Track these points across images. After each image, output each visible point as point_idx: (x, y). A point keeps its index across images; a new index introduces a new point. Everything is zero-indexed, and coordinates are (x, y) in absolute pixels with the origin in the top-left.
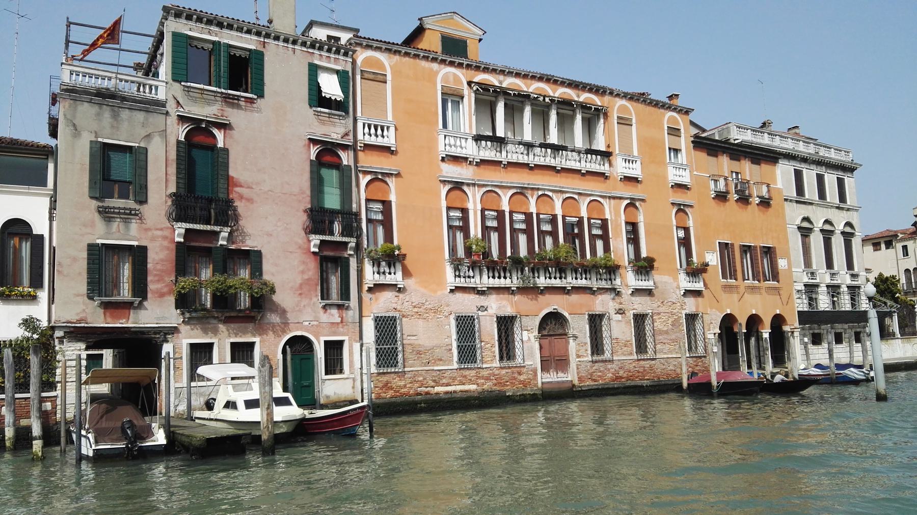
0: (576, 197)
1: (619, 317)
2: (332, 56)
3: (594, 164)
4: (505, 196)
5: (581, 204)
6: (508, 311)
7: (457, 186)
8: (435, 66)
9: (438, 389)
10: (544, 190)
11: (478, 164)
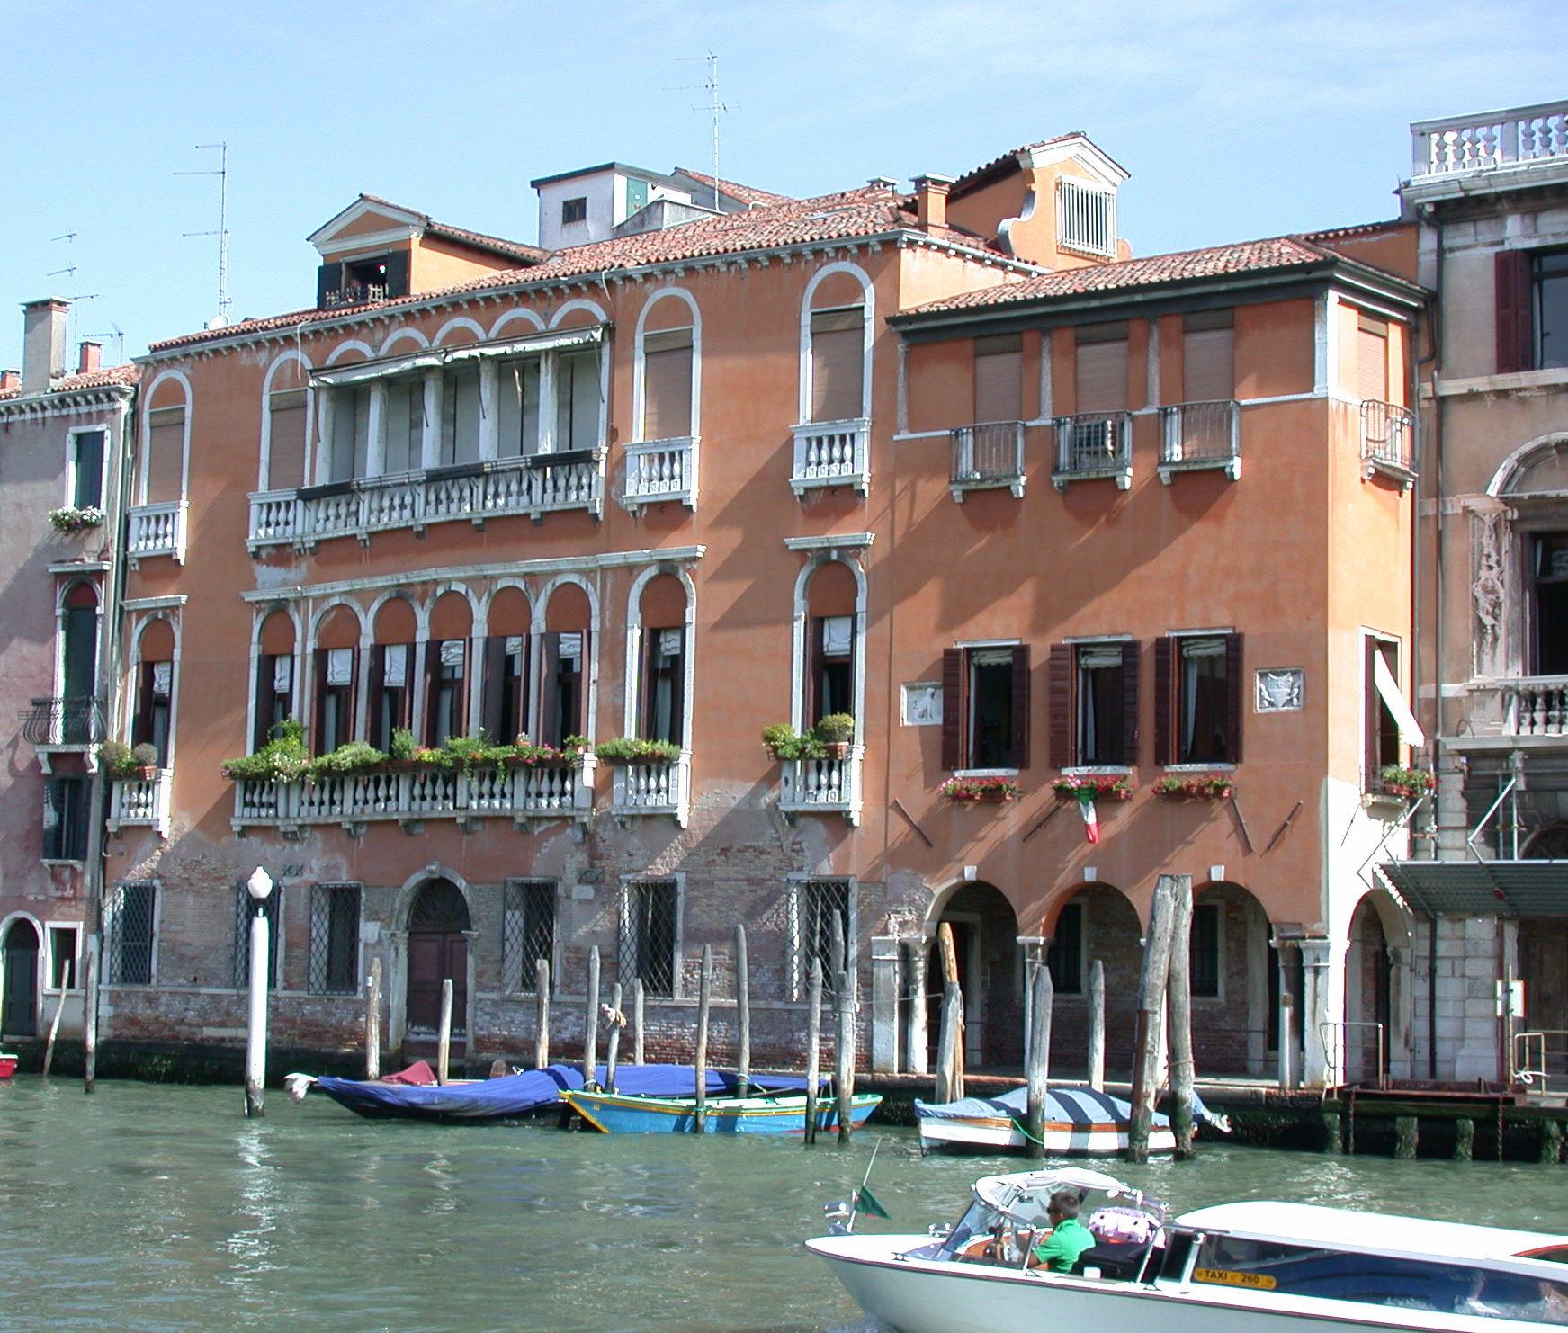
0: (521, 585)
1: (588, 892)
2: (94, 408)
3: (542, 498)
4: (366, 611)
5: (533, 600)
6: (344, 878)
7: (278, 611)
8: (263, 357)
9: (210, 1032)
10: (449, 581)
11: (313, 551)
